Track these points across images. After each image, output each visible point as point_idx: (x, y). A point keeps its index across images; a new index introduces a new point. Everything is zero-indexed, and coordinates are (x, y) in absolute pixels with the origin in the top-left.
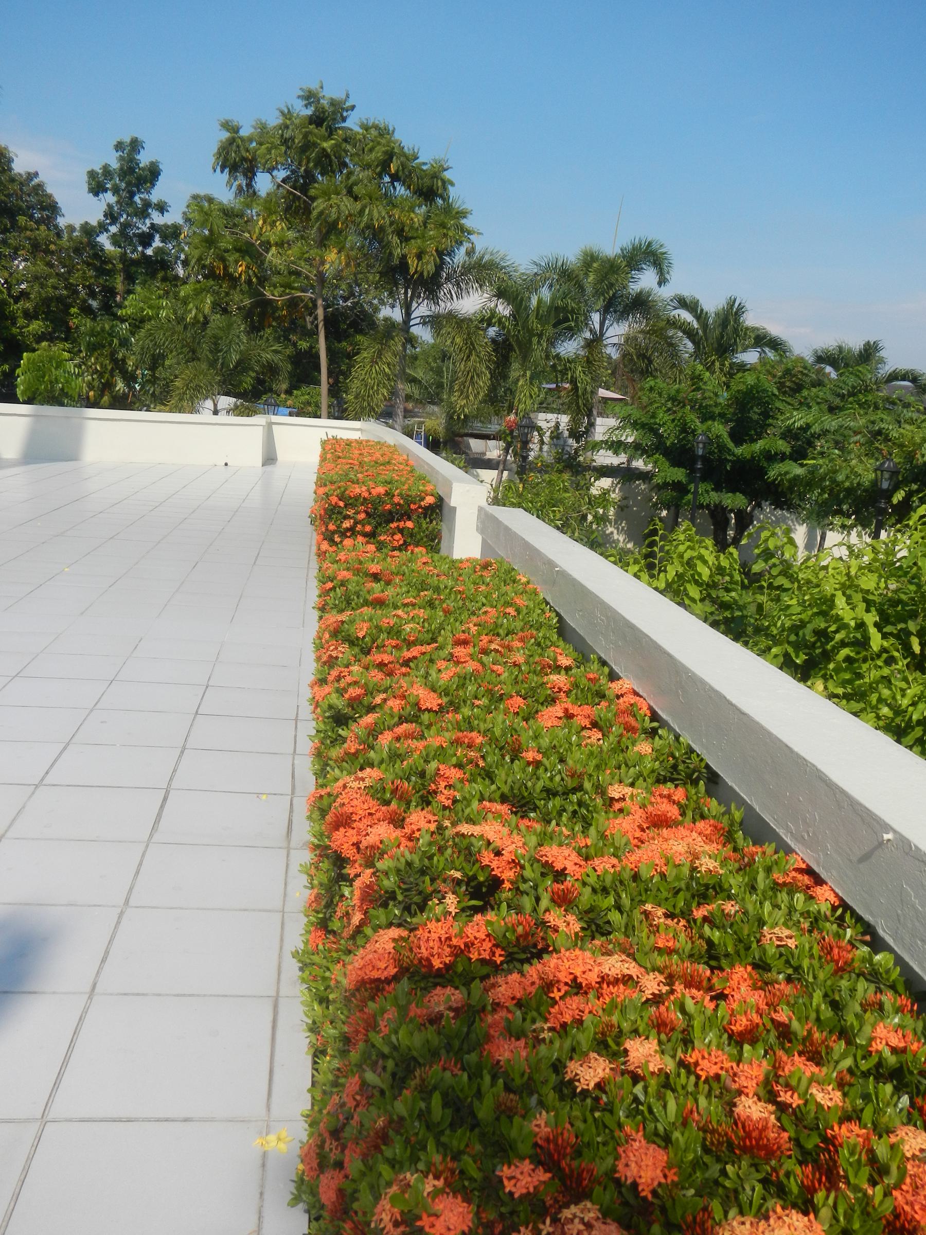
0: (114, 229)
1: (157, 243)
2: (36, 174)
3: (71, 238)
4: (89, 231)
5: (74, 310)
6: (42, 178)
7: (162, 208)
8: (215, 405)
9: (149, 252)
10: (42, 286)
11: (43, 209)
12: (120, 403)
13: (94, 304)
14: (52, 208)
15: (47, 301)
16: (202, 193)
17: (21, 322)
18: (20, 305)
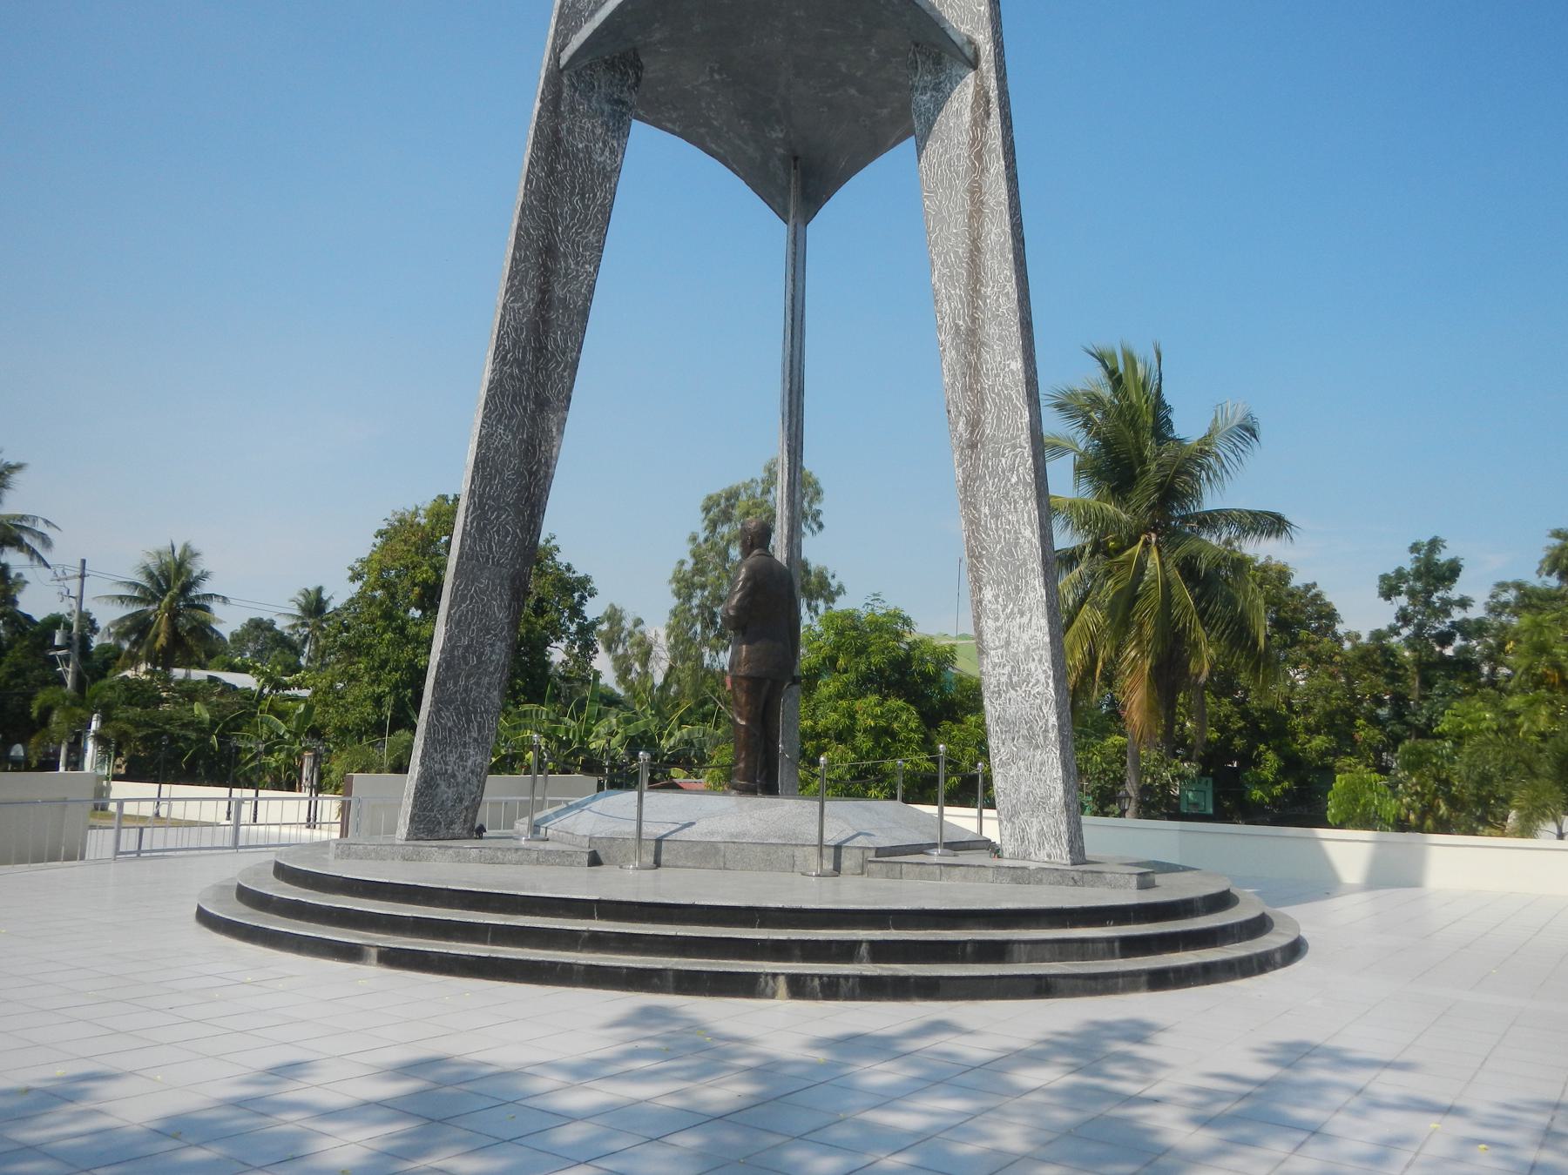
0: (1406, 632)
1: (1458, 641)
2: (1315, 585)
3: (1355, 647)
4: (1378, 636)
5: (1360, 722)
6: (1320, 587)
7: (1464, 603)
8: (1560, 828)
9: (1449, 651)
10: (1327, 699)
11: (1320, 618)
12: (1443, 827)
13: (1383, 712)
14: (1329, 616)
15: (1330, 715)
16: (1509, 580)
17: (1302, 737)
18: (1301, 720)
